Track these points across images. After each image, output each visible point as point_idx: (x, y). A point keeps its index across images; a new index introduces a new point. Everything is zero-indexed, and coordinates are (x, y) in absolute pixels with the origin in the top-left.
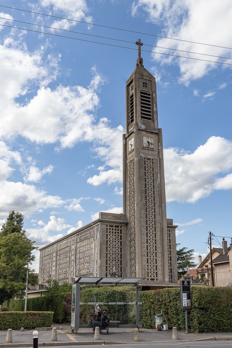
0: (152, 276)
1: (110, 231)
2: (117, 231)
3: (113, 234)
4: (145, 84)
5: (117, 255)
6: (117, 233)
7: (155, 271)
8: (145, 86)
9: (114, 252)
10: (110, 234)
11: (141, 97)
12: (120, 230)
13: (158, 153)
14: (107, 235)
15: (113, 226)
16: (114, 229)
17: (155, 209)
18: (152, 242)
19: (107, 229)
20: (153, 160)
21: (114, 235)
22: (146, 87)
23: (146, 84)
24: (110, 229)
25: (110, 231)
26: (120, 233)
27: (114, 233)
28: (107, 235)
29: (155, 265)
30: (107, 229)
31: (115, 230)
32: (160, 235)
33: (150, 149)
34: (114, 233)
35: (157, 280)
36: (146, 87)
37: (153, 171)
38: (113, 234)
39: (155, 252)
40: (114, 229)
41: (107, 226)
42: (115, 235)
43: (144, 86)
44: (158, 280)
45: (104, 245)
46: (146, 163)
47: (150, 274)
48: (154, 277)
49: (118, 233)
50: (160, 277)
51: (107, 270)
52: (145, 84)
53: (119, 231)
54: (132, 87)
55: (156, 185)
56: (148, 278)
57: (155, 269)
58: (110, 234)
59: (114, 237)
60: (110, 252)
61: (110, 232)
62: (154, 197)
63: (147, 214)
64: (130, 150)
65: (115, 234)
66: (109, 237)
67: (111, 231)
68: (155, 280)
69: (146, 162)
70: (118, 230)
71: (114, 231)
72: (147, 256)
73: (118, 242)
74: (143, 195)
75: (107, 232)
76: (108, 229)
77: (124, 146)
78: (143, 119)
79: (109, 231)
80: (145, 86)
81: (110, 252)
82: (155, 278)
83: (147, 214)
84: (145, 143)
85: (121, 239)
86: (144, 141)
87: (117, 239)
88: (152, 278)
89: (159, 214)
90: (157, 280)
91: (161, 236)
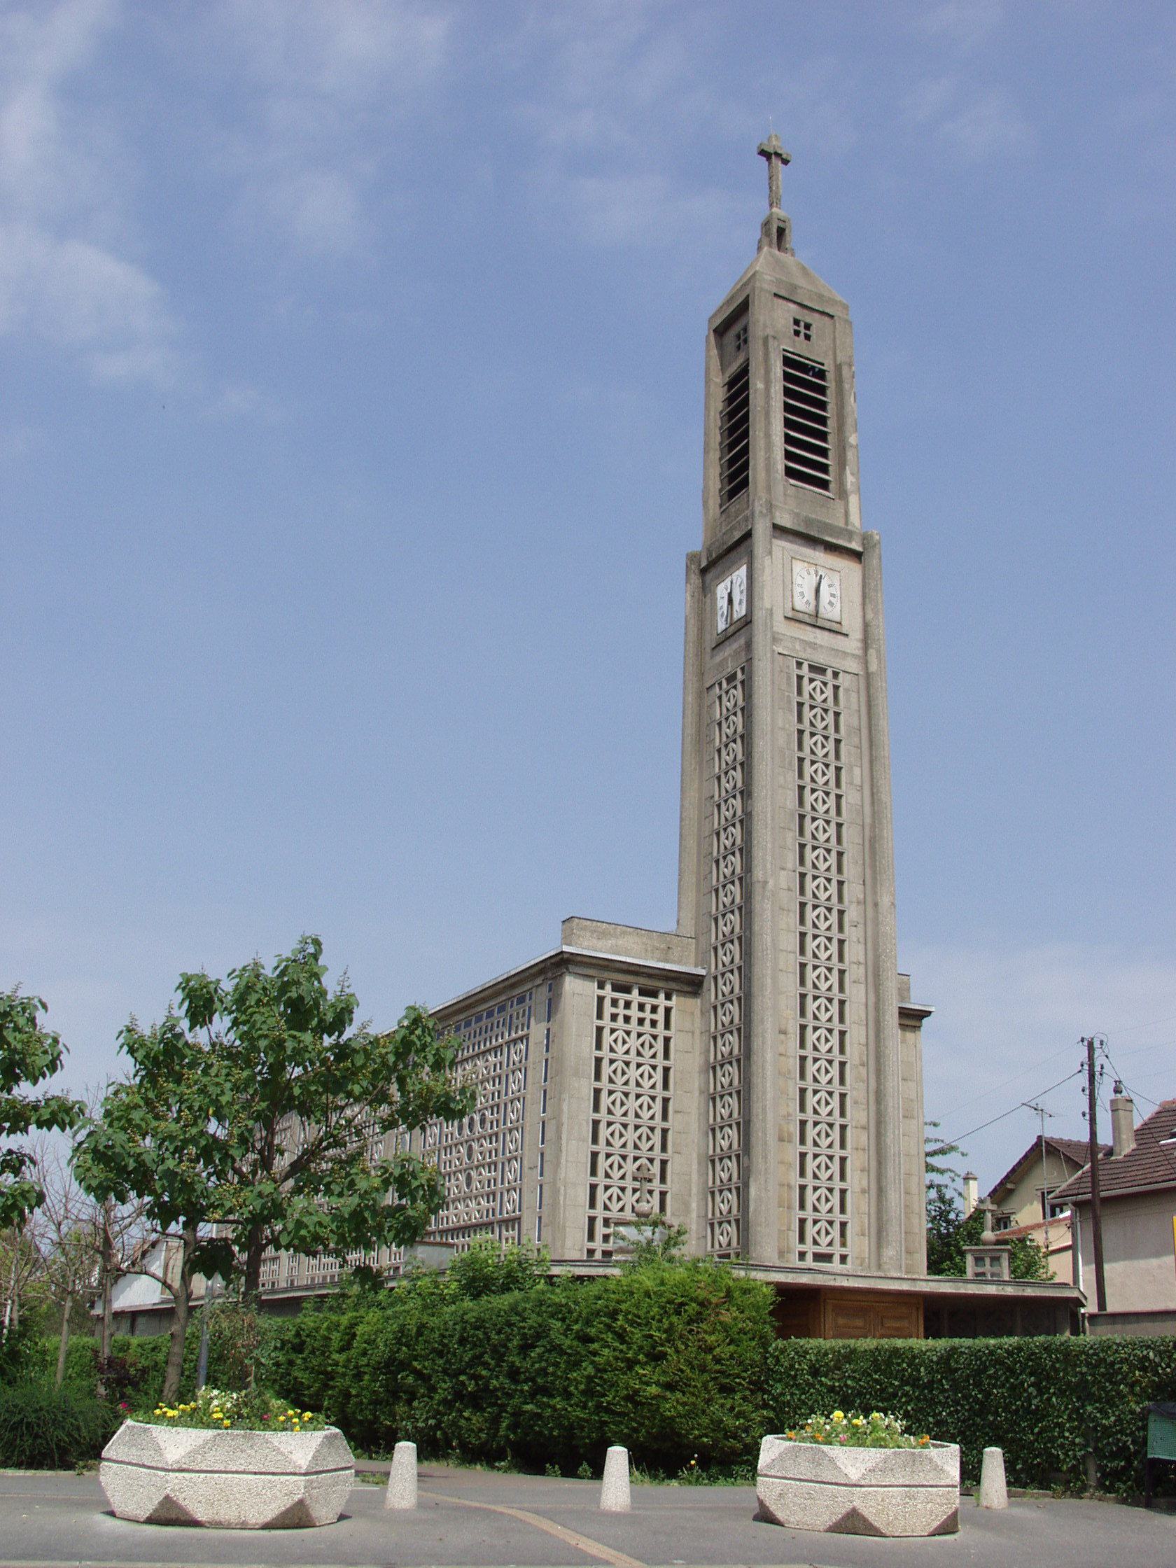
0: (824, 1241)
1: (614, 1010)
2: (647, 1015)
3: (627, 1027)
4: (802, 324)
5: (645, 1099)
6: (647, 1023)
7: (837, 1185)
8: (802, 335)
9: (631, 1114)
10: (614, 1025)
11: (785, 395)
12: (661, 1011)
13: (859, 645)
14: (600, 1030)
15: (627, 990)
16: (635, 1006)
17: (841, 913)
18: (826, 889)
19: (601, 1000)
20: (836, 675)
21: (633, 1035)
22: (808, 337)
23: (808, 327)
24: (614, 1003)
25: (614, 1010)
26: (661, 1024)
27: (634, 1021)
28: (600, 1030)
29: (837, 1185)
30: (601, 1000)
31: (641, 1007)
32: (863, 1041)
33: (827, 625)
34: (634, 1021)
35: (843, 1259)
36: (808, 337)
37: (837, 729)
38: (627, 1027)
39: (838, 1058)
40: (635, 1006)
41: (601, 986)
42: (640, 1035)
43: (797, 333)
44: (849, 1259)
45: (584, 1082)
46: (807, 688)
47: (810, 1231)
48: (830, 1244)
49: (654, 1023)
50: (858, 1245)
51: (592, 1204)
52: (802, 324)
53: (660, 1016)
54: (738, 337)
55: (849, 797)
56: (802, 1248)
57: (837, 1209)
58: (614, 1025)
59: (633, 1043)
60: (610, 1177)
61: (614, 1017)
62: (840, 970)
63: (803, 935)
64: (721, 626)
65: (640, 1029)
66: (607, 1039)
67: (621, 1011)
68: (837, 1258)
69: (806, 681)
70: (654, 1009)
71: (634, 1013)
72: (803, 1141)
73: (654, 1067)
74: (789, 841)
75: (600, 1016)
76: (607, 1003)
77: (692, 651)
78: (792, 481)
79: (608, 1010)
80: (802, 335)
81: (610, 1177)
82: (837, 1250)
83: (803, 935)
84: (802, 593)
85: (666, 1055)
86: (798, 580)
87: (647, 1053)
88: (823, 1249)
89: (862, 940)
90: (843, 1259)
91: (867, 1044)
